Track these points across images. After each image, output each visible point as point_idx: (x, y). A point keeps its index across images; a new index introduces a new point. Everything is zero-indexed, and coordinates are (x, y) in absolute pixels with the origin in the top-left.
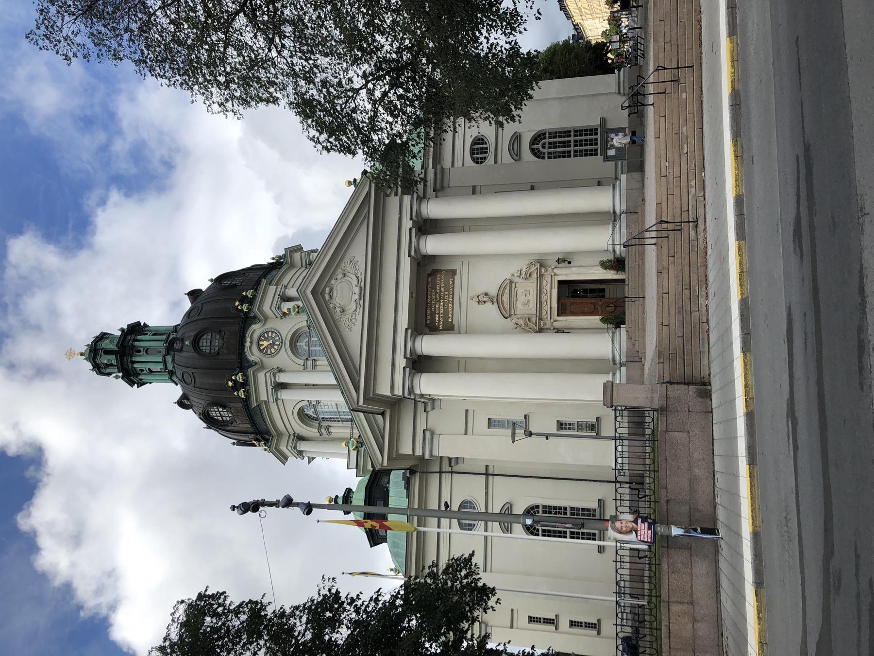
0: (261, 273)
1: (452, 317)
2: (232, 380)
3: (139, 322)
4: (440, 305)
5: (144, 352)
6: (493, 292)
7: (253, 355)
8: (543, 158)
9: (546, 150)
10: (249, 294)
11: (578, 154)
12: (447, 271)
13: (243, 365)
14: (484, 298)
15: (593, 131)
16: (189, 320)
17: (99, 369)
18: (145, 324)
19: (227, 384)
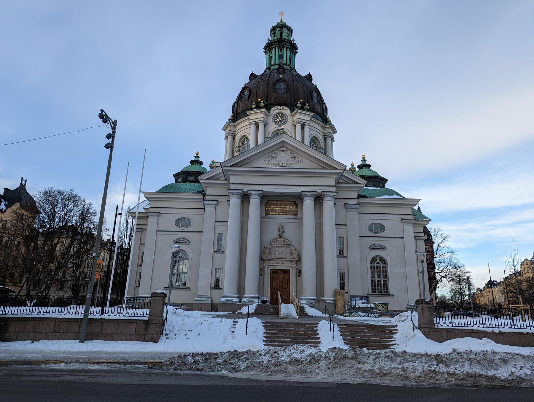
0: (320, 112)
1: (272, 214)
2: (261, 100)
3: (298, 49)
4: (278, 208)
5: (281, 53)
6: (285, 235)
8: (371, 263)
9: (376, 265)
10: (307, 107)
11: (373, 282)
12: (297, 211)
13: (268, 107)
14: (281, 230)
15: (386, 290)
16: (294, 76)
17: (273, 30)
18: (298, 52)
19: (259, 98)
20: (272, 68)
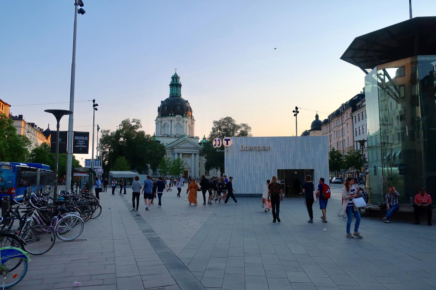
7: (177, 116)
13: (175, 115)
20: (173, 95)
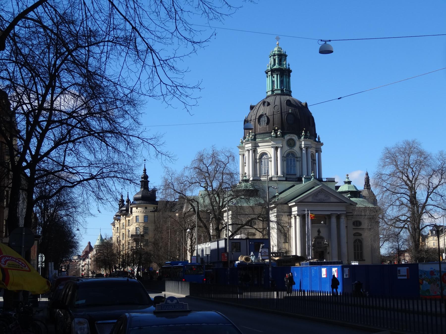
7: (287, 137)
8: (354, 243)
9: (356, 244)
11: (355, 253)
20: (276, 92)
